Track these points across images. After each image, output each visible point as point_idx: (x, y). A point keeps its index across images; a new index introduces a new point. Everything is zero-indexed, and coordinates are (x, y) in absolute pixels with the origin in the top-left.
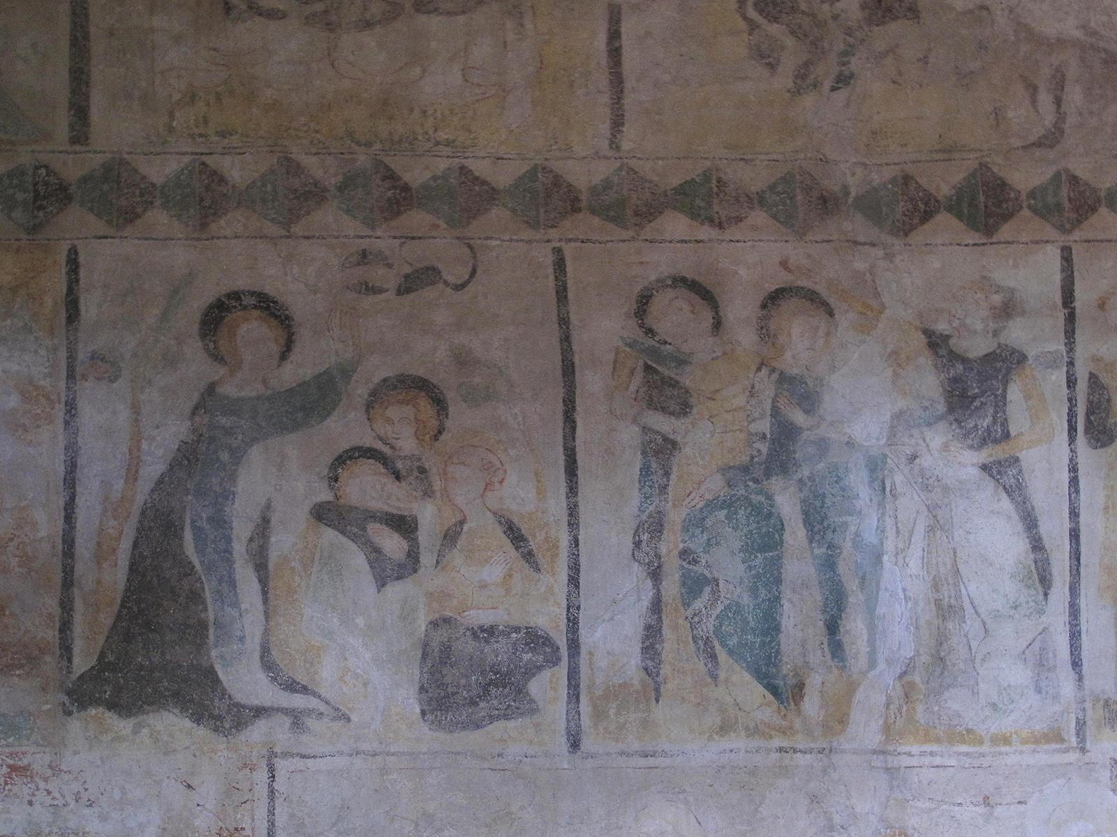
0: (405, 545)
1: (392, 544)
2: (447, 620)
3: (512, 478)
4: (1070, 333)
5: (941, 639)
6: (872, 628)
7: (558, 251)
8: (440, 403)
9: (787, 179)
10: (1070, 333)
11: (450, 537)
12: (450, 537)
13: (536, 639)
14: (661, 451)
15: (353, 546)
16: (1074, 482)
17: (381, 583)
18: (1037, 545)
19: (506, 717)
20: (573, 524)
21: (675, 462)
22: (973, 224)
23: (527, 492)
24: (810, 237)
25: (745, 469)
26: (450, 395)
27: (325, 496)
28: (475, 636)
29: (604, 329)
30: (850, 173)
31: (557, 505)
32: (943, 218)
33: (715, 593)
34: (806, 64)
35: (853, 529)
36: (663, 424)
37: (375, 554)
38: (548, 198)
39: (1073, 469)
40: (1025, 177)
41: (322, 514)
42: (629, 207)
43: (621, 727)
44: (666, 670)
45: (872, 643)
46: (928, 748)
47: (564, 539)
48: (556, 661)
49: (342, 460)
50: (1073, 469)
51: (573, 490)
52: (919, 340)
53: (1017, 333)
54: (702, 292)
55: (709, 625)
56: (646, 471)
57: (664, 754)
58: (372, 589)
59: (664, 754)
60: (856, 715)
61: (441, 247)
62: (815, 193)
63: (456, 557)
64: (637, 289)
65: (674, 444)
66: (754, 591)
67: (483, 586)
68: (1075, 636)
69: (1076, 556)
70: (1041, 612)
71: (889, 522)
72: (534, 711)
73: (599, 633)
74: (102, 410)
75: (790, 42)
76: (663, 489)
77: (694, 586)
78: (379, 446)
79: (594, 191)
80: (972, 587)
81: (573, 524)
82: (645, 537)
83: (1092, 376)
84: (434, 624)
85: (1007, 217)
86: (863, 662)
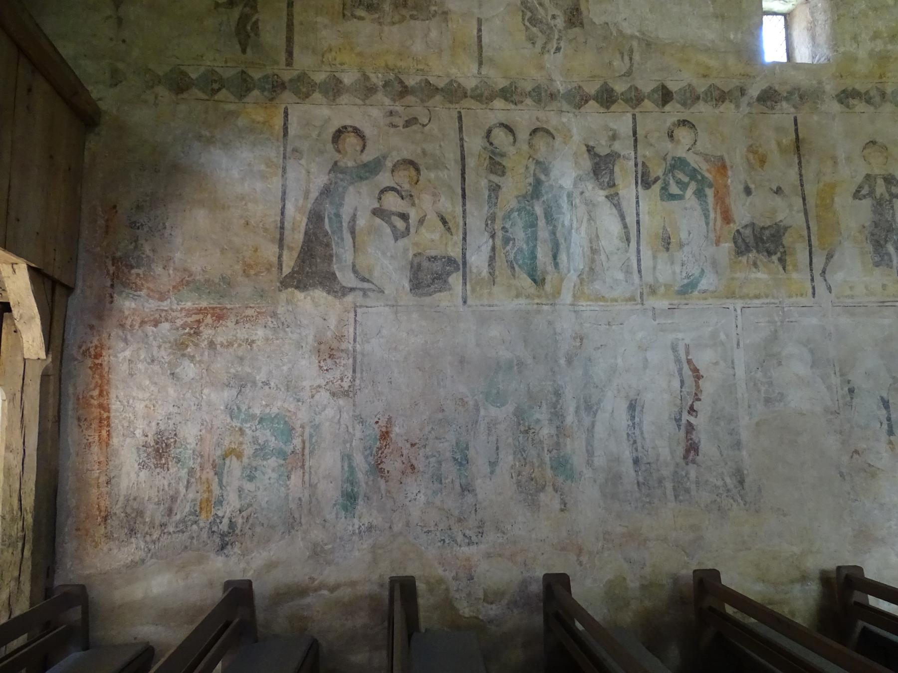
0: (405, 225)
1: (400, 224)
2: (420, 254)
3: (443, 199)
4: (635, 147)
5: (593, 261)
7: (459, 112)
8: (417, 170)
9: (538, 87)
10: (635, 147)
11: (421, 221)
12: (421, 221)
13: (450, 261)
14: (495, 189)
15: (384, 224)
16: (637, 202)
18: (625, 226)
19: (440, 291)
20: (464, 217)
21: (500, 193)
22: (602, 105)
23: (449, 205)
24: (547, 109)
25: (524, 197)
28: (429, 260)
29: (475, 143)
30: (560, 85)
31: (459, 210)
32: (592, 103)
33: (514, 243)
34: (546, 43)
35: (561, 219)
36: (495, 179)
37: (394, 228)
38: (454, 93)
39: (637, 198)
40: (620, 87)
42: (484, 96)
44: (497, 273)
46: (589, 303)
47: (461, 223)
50: (637, 198)
51: (464, 204)
52: (585, 148)
53: (617, 146)
54: (509, 128)
55: (512, 256)
56: (489, 196)
57: (497, 305)
59: (497, 305)
60: (564, 291)
61: (418, 110)
63: (423, 230)
65: (499, 187)
66: (528, 244)
67: (433, 241)
68: (639, 261)
69: (639, 231)
70: (627, 251)
72: (450, 289)
73: (473, 258)
75: (540, 34)
76: (496, 204)
77: (506, 241)
78: (396, 186)
81: (464, 217)
82: (489, 222)
83: (643, 163)
84: (415, 255)
85: (613, 102)
86: (565, 271)
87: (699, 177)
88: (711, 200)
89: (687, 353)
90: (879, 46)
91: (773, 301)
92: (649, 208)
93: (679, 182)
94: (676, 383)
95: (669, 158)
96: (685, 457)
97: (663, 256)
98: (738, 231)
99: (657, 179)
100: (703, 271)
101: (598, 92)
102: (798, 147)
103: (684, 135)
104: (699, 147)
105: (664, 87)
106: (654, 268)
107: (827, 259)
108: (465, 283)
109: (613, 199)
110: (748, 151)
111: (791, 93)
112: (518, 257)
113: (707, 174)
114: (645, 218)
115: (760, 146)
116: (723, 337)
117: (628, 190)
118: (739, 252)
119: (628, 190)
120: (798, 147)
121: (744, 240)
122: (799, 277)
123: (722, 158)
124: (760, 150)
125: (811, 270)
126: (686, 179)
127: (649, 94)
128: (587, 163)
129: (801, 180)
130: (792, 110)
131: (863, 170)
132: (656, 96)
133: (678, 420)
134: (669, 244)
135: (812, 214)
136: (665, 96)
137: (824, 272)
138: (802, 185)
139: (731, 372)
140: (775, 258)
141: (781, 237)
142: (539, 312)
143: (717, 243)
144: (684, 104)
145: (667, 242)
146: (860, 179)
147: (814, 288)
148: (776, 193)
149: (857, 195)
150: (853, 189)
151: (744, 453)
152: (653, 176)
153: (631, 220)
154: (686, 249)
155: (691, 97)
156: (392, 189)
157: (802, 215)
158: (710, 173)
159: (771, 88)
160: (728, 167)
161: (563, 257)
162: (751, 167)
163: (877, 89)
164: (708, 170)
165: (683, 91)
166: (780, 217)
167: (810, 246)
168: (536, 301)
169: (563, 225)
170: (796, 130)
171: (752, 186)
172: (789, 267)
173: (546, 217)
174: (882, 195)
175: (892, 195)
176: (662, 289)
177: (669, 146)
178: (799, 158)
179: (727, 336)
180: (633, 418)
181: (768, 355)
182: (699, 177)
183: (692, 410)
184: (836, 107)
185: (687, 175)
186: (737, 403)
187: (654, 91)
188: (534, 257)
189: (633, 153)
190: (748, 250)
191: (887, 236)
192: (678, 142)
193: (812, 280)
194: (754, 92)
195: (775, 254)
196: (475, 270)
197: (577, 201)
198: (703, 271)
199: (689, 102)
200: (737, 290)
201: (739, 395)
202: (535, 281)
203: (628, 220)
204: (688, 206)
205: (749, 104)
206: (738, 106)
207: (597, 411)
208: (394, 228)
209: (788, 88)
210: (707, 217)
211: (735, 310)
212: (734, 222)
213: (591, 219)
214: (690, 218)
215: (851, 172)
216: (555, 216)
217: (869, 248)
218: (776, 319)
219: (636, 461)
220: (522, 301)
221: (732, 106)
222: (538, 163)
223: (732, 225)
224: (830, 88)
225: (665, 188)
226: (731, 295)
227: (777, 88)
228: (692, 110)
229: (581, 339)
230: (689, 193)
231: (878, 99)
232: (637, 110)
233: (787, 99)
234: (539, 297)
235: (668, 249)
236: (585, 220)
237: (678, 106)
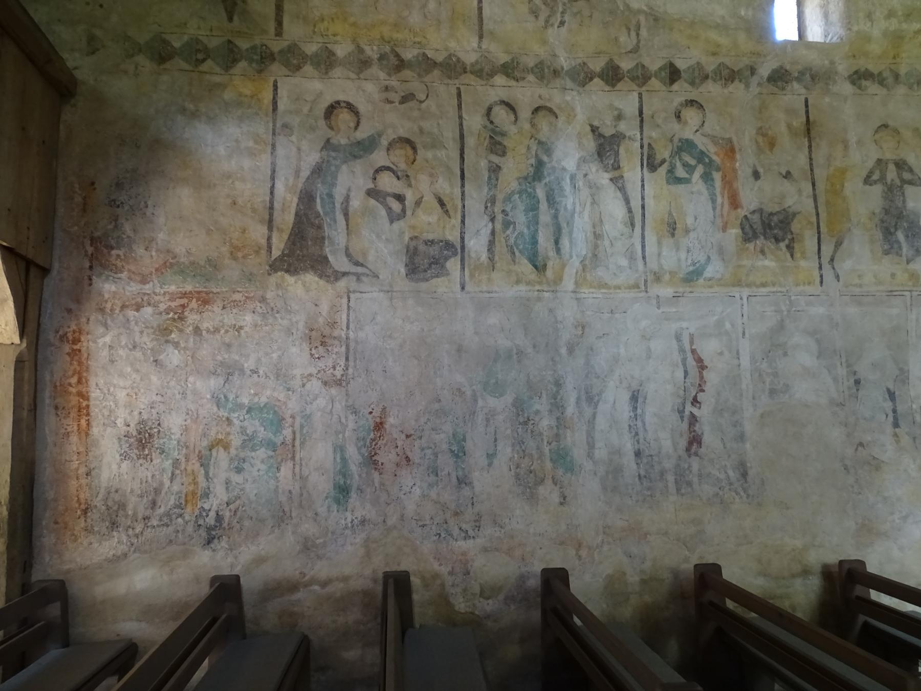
1: (396, 206)
2: (416, 237)
3: (441, 180)
4: (641, 127)
5: (596, 246)
6: (571, 242)
7: (458, 89)
8: (414, 149)
9: (542, 63)
10: (641, 127)
11: (418, 203)
12: (418, 203)
13: (448, 245)
14: (495, 170)
15: (379, 205)
16: (643, 186)
17: (392, 222)
18: (630, 211)
19: (437, 277)
20: (463, 199)
21: (500, 175)
22: (607, 82)
23: (447, 187)
24: (550, 86)
25: (526, 178)
26: (419, 146)
27: (371, 186)
28: (426, 244)
29: (474, 122)
30: (564, 62)
31: (457, 191)
33: (514, 228)
35: (564, 203)
36: (495, 159)
37: (389, 210)
38: (452, 68)
39: (643, 181)
40: (625, 65)
41: (370, 193)
42: (484, 71)
43: (480, 281)
44: (497, 258)
45: (571, 248)
46: (592, 290)
48: (455, 254)
49: (377, 171)
50: (643, 181)
51: (463, 186)
52: (588, 128)
53: (622, 127)
54: (510, 106)
55: (512, 240)
56: (489, 178)
57: (496, 292)
58: (387, 224)
59: (496, 292)
60: (565, 277)
62: (552, 69)
63: (419, 212)
64: (487, 105)
66: (529, 228)
67: (429, 224)
68: (643, 247)
69: (643, 215)
70: (631, 237)
71: (577, 200)
72: (448, 274)
73: (472, 243)
74: (285, 149)
77: (507, 224)
78: (392, 166)
79: (472, 65)
80: (607, 227)
81: (463, 199)
83: (649, 144)
84: (411, 239)
85: (619, 80)
86: (567, 256)
87: (707, 160)
88: (718, 183)
89: (692, 343)
90: (894, 25)
91: (779, 289)
92: (654, 192)
93: (685, 165)
94: (680, 374)
95: (676, 140)
96: (688, 450)
97: (668, 242)
98: (745, 216)
99: (663, 162)
100: (709, 258)
101: (603, 70)
102: (808, 130)
103: (692, 116)
104: (707, 129)
105: (672, 65)
106: (659, 255)
107: (836, 246)
108: (463, 268)
109: (618, 181)
110: (757, 134)
111: (802, 73)
112: (519, 242)
113: (714, 158)
114: (650, 202)
115: (770, 128)
116: (728, 326)
117: (633, 173)
118: (747, 239)
119: (633, 173)
120: (808, 130)
121: (751, 227)
122: (807, 265)
123: (730, 141)
124: (770, 133)
125: (820, 258)
126: (693, 162)
127: (656, 72)
128: (591, 144)
129: (811, 165)
130: (803, 91)
131: (874, 154)
132: (663, 74)
133: (681, 412)
134: (674, 229)
135: (821, 200)
136: (673, 74)
137: (832, 260)
138: (812, 170)
139: (736, 362)
140: (783, 245)
141: (789, 224)
142: (539, 299)
143: (724, 229)
144: (692, 83)
145: (672, 228)
146: (870, 164)
147: (821, 276)
148: (785, 177)
149: (867, 180)
150: (864, 174)
151: (748, 446)
152: (659, 158)
153: (636, 204)
154: (692, 235)
155: (700, 76)
156: (388, 169)
157: (811, 201)
158: (718, 156)
159: (781, 67)
160: (737, 150)
161: (565, 242)
162: (760, 150)
163: (891, 70)
164: (716, 153)
165: (691, 69)
166: (789, 202)
167: (819, 233)
168: (537, 287)
169: (566, 209)
170: (807, 112)
171: (761, 170)
172: (798, 255)
173: (548, 200)
174: (892, 180)
175: (904, 182)
176: (667, 277)
177: (676, 126)
178: (810, 141)
179: (733, 325)
180: (635, 409)
181: (774, 345)
182: (707, 160)
183: (695, 401)
184: (847, 88)
185: (694, 158)
186: (741, 395)
187: (661, 69)
188: (535, 242)
189: (639, 134)
190: (755, 236)
191: (896, 223)
192: (686, 123)
193: (820, 268)
194: (764, 71)
195: (783, 240)
196: (473, 255)
197: (580, 183)
198: (709, 258)
199: (697, 81)
200: (744, 278)
201: (744, 386)
202: (536, 267)
203: (632, 204)
204: (694, 189)
205: (759, 84)
206: (747, 86)
207: (598, 401)
208: (389, 210)
209: (800, 67)
210: (714, 201)
211: (741, 299)
212: (742, 208)
213: (594, 203)
214: (696, 203)
215: (861, 157)
216: (558, 199)
217: (879, 235)
218: (784, 308)
219: (638, 454)
220: (522, 288)
221: (742, 86)
222: (540, 143)
223: (739, 210)
224: (843, 68)
225: (671, 171)
226: (738, 283)
227: (788, 68)
228: (700, 90)
229: (583, 327)
230: (696, 176)
231: (890, 80)
232: (644, 88)
233: (798, 79)
234: (540, 283)
235: (673, 235)
236: (588, 204)
237: (686, 85)
